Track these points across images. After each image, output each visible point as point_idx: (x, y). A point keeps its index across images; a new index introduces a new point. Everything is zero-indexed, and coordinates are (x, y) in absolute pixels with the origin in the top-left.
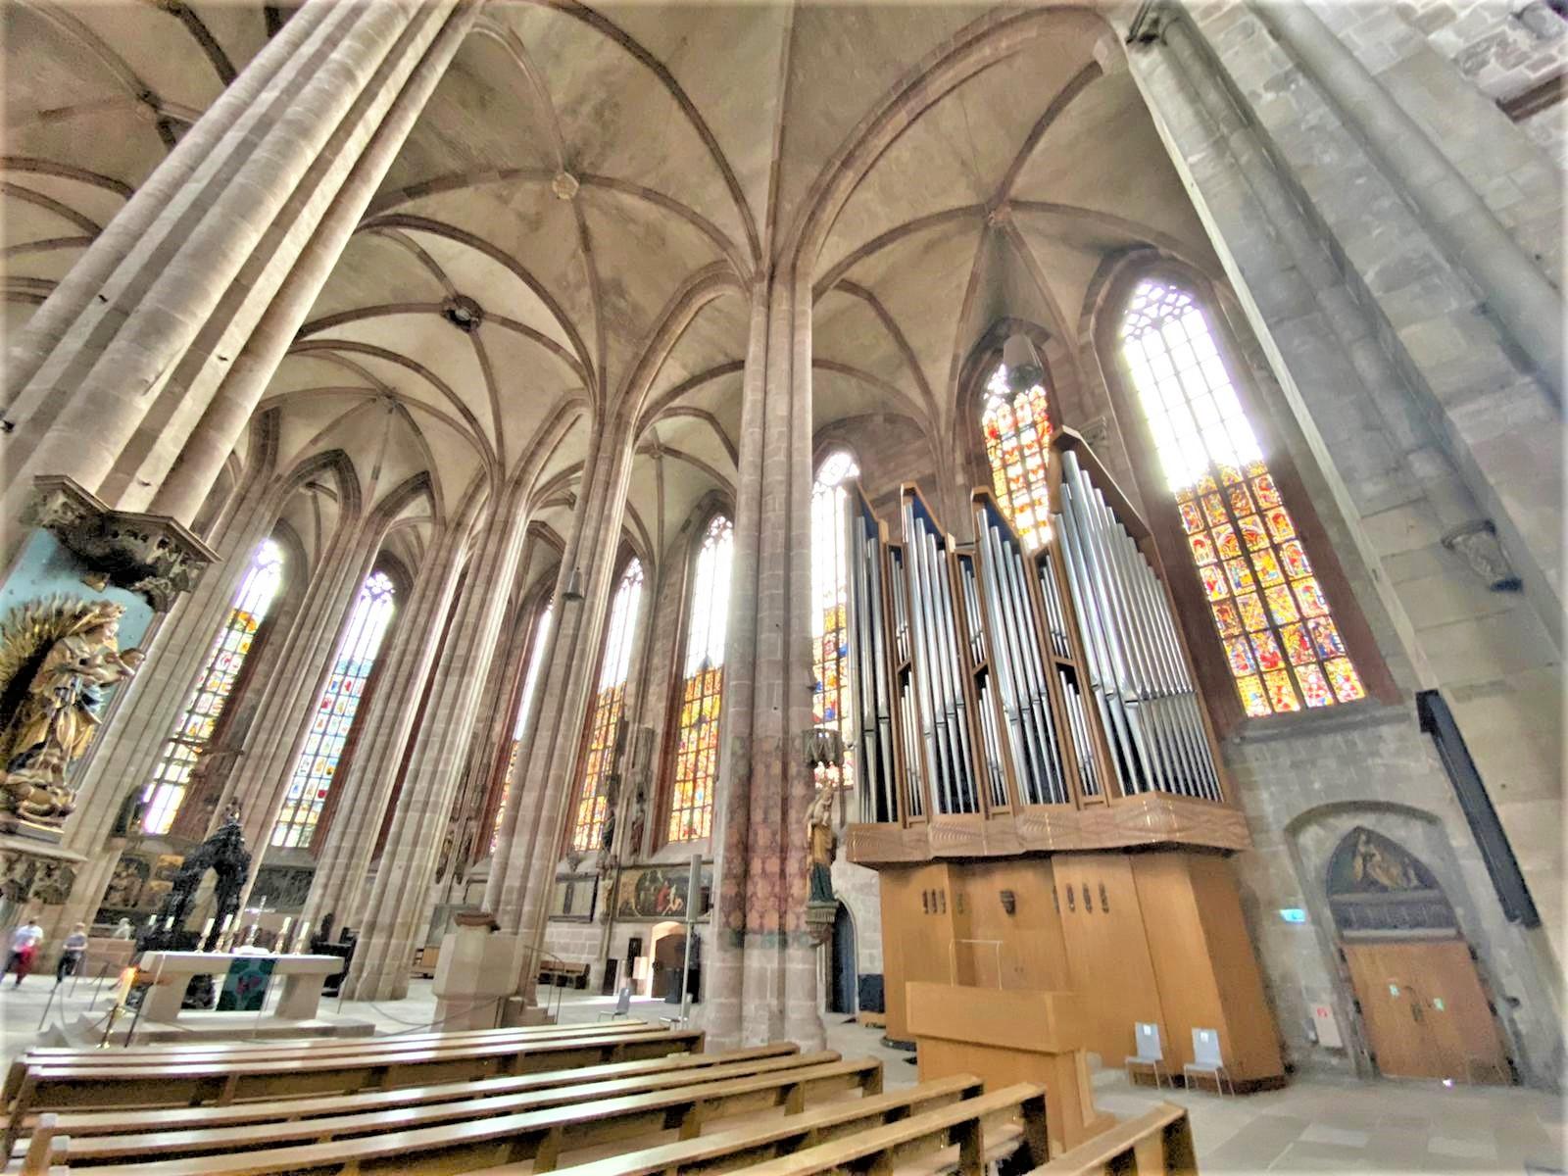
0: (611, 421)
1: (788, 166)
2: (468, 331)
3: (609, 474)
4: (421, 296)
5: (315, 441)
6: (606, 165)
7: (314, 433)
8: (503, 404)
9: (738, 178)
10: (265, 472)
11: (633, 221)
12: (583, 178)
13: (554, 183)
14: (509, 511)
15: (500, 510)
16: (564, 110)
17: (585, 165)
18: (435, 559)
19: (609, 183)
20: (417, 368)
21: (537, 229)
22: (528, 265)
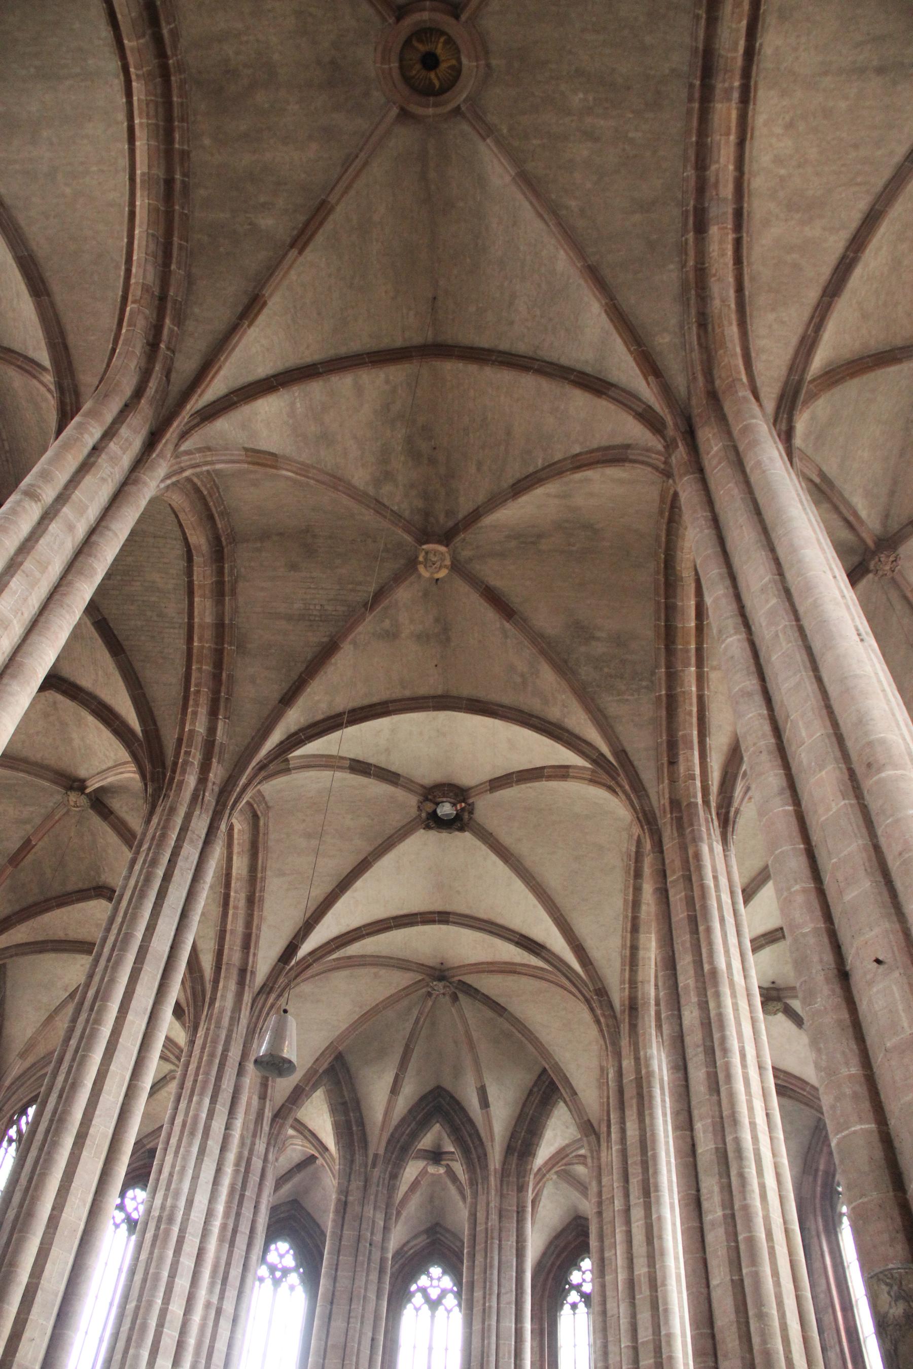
0: (666, 823)
1: (629, 299)
2: (461, 829)
3: (690, 902)
4: (396, 820)
5: (395, 1089)
6: (462, 500)
7: (388, 1079)
8: (560, 900)
9: (588, 370)
10: (358, 1158)
11: (540, 536)
12: (447, 538)
13: (421, 569)
14: (637, 1059)
15: (625, 1063)
16: (377, 483)
17: (444, 522)
18: (600, 1194)
19: (475, 516)
20: (442, 917)
21: (448, 639)
22: (466, 691)
